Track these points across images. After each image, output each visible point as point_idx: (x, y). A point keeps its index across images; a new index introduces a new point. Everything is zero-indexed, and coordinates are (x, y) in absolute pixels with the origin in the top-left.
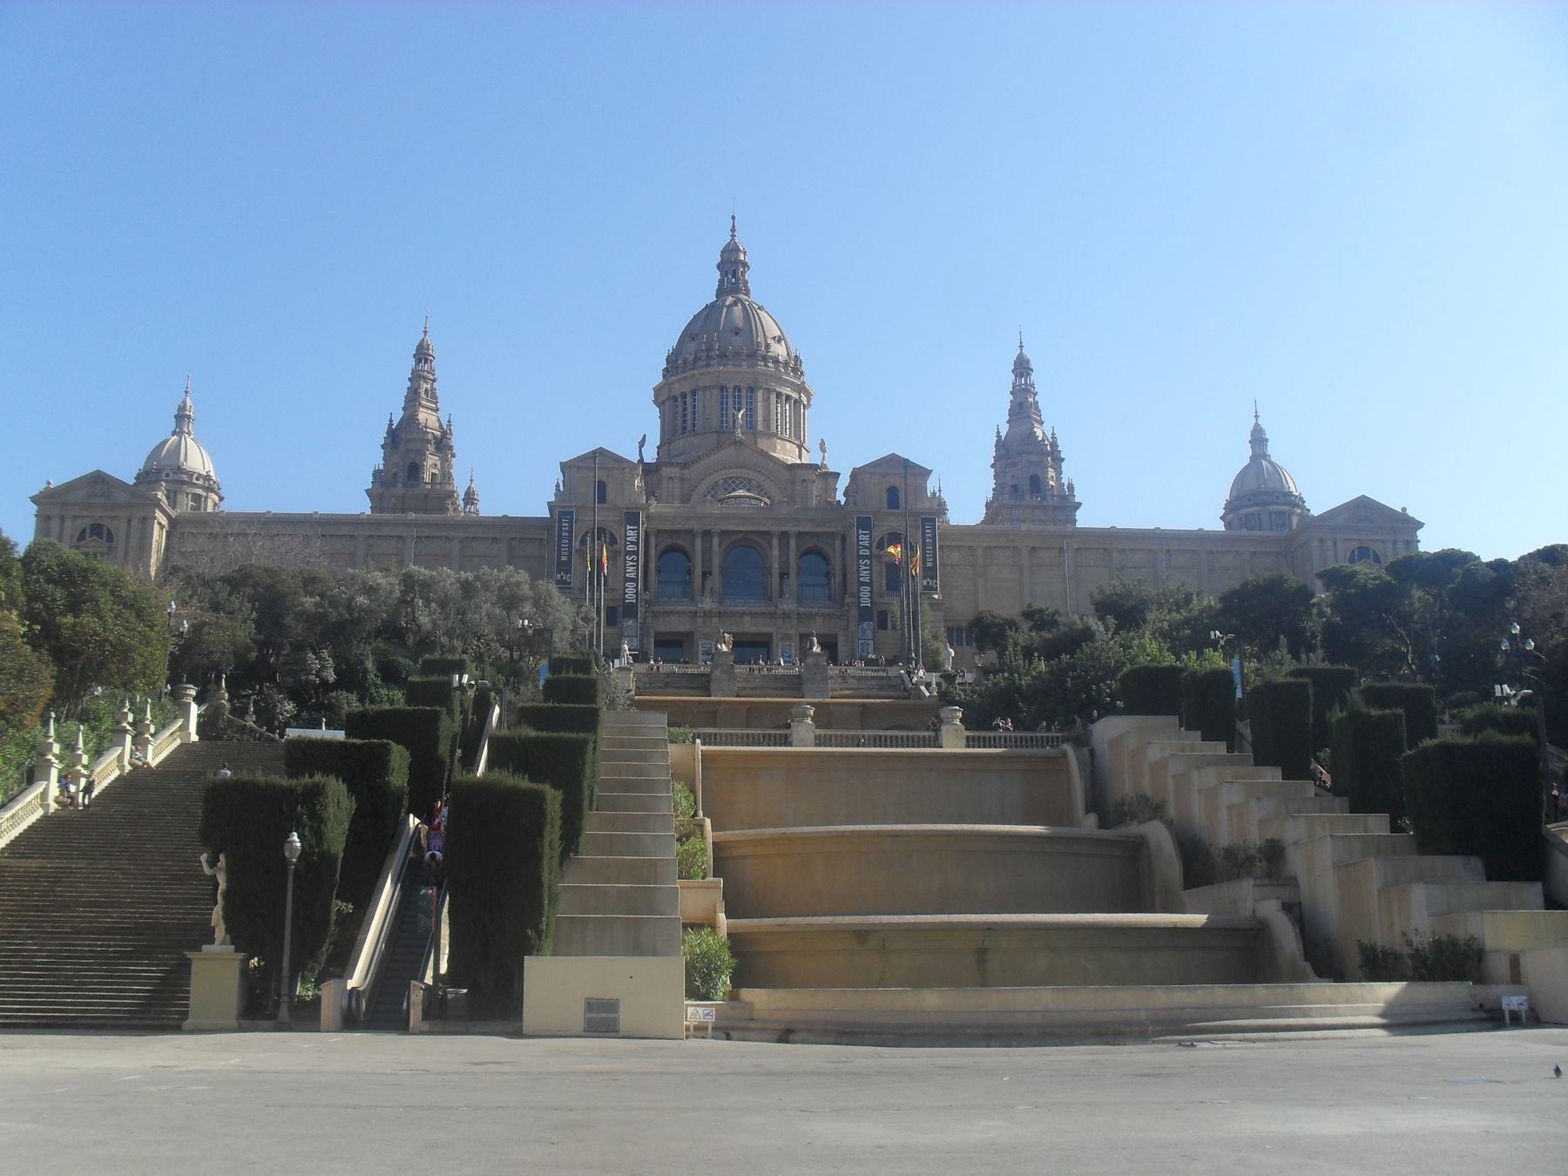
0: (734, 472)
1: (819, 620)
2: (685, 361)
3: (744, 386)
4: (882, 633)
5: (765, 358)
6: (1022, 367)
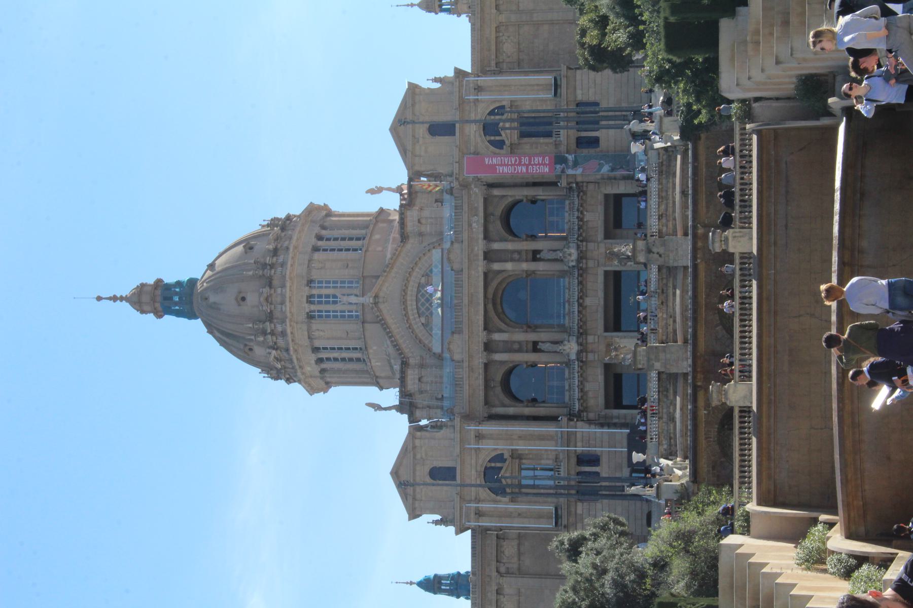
1: (588, 216)
2: (278, 359)
3: (306, 291)
4: (603, 144)
5: (272, 266)
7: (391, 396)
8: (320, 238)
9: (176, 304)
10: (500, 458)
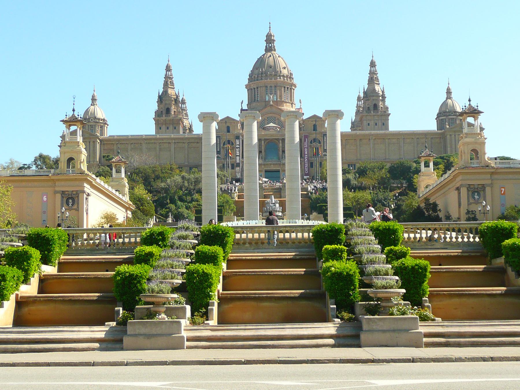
0: (270, 115)
2: (254, 77)
3: (273, 86)
5: (280, 76)
6: (373, 64)
7: (245, 107)
8: (288, 88)
9: (269, 45)
10: (233, 144)
